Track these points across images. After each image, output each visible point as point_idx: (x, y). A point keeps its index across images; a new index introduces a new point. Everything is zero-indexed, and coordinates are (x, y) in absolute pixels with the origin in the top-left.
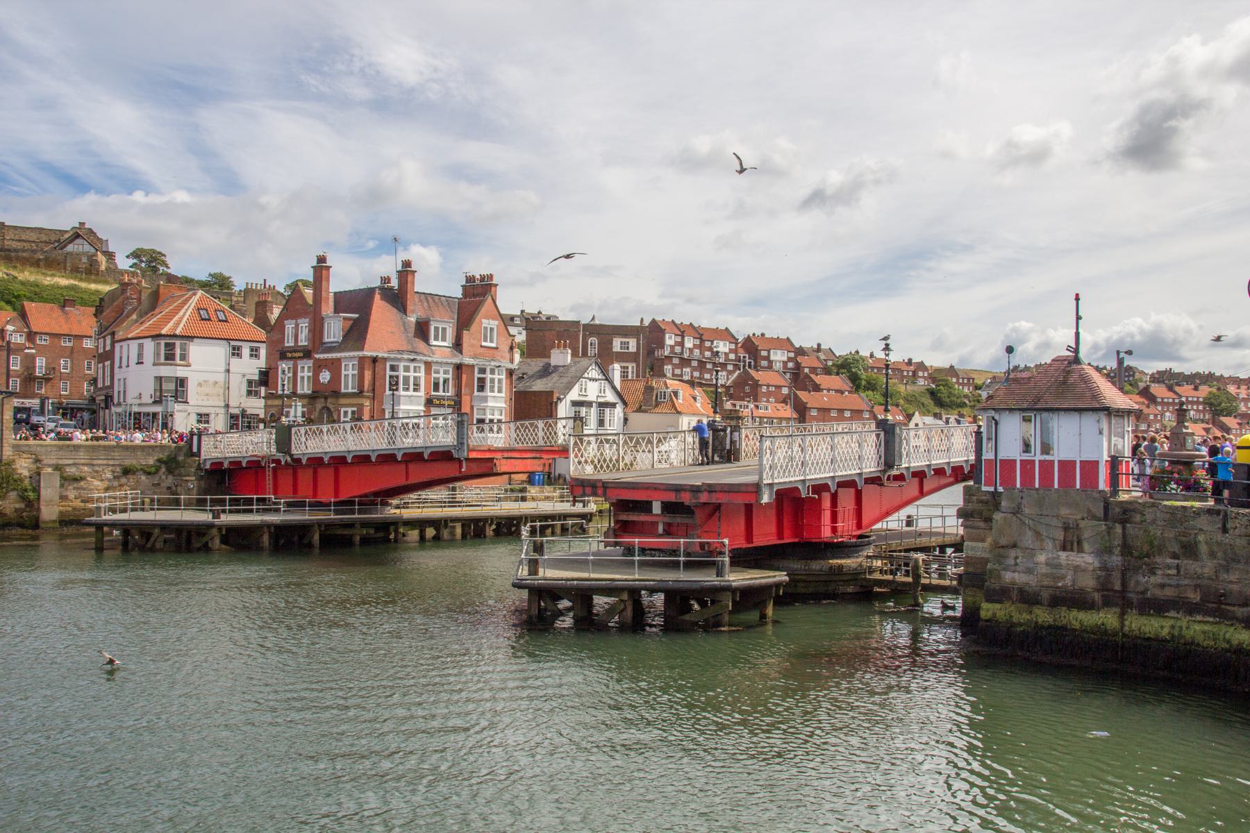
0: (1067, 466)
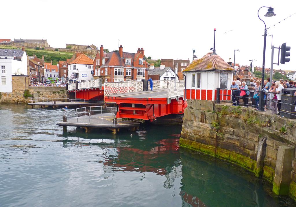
0: (204, 91)
